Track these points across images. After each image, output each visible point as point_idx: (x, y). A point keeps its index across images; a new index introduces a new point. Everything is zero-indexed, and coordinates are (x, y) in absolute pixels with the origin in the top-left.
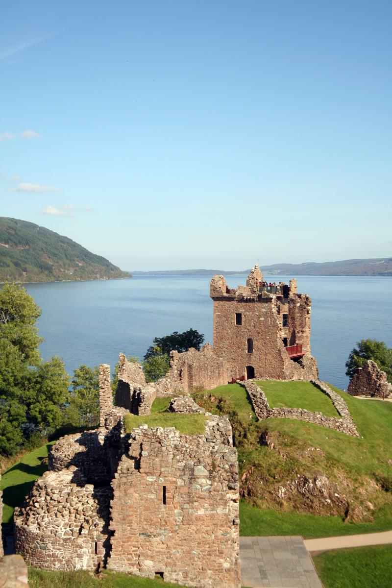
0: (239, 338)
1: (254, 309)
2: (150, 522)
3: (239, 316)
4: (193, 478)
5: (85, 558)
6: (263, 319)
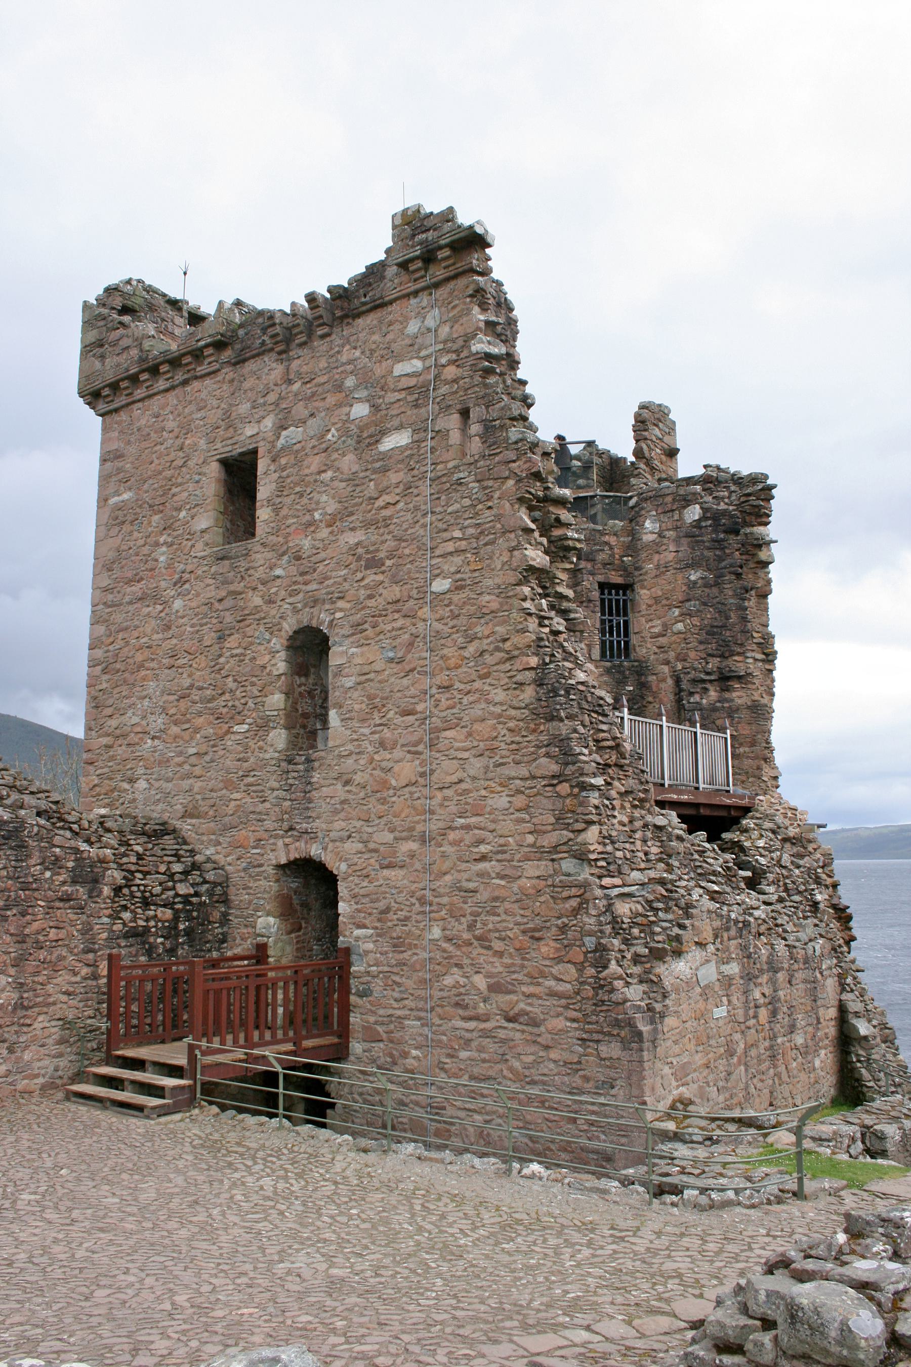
1: (339, 387)
3: (240, 475)
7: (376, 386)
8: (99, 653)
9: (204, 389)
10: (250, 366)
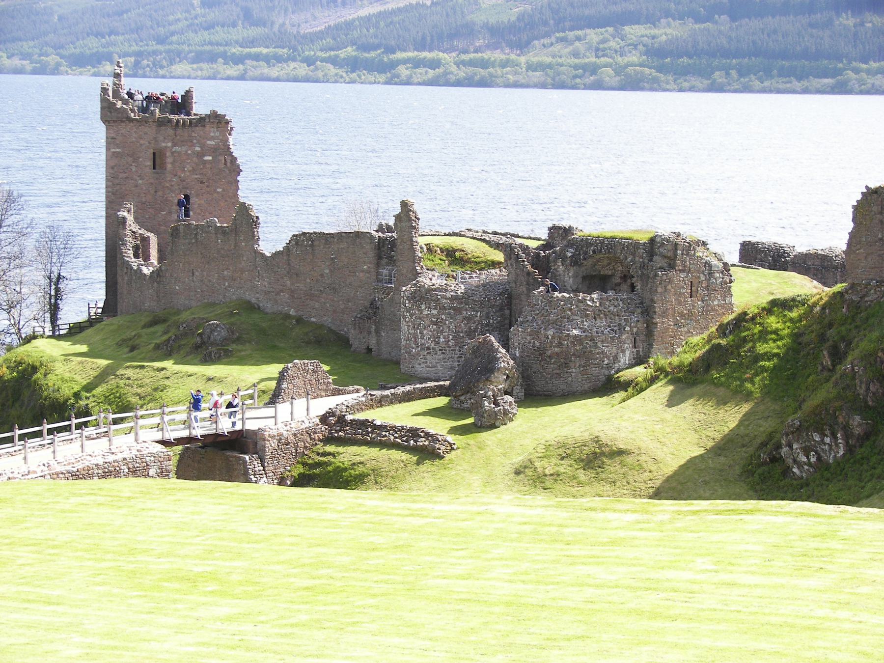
0: (160, 193)
2: (682, 315)
4: (711, 274)
5: (628, 353)
6: (210, 158)
7: (203, 146)
8: (110, 189)
9: (147, 129)
10: (163, 128)
